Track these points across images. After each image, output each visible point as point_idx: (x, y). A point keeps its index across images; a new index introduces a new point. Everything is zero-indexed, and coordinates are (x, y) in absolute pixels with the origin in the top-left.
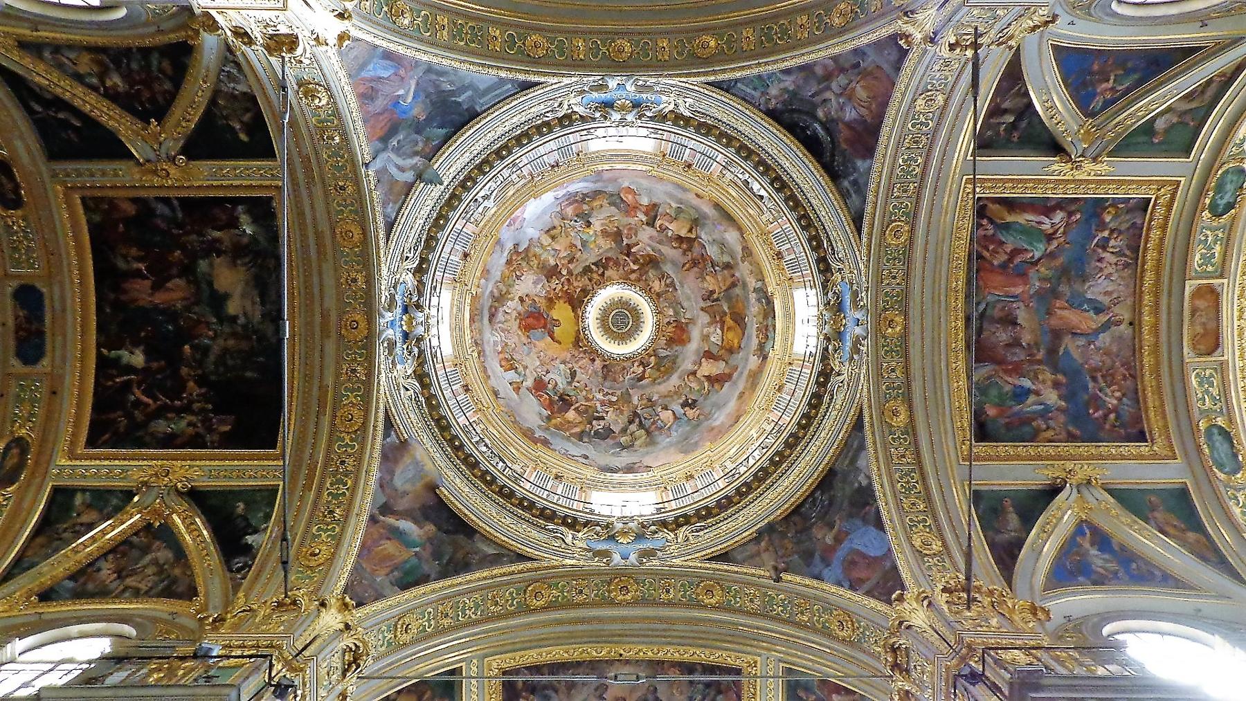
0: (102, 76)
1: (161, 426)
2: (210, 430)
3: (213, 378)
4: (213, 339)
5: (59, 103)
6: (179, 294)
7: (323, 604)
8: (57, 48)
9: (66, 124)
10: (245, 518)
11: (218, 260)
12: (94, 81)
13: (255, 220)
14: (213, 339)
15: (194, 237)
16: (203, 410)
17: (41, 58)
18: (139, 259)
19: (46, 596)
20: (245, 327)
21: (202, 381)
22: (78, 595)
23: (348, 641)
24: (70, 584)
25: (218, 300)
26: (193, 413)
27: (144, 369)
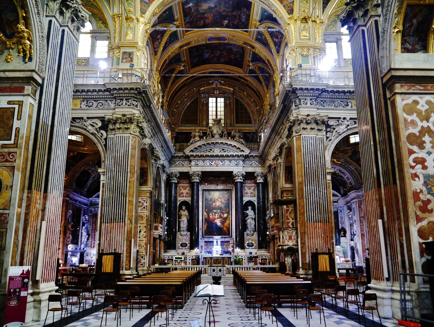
0: (158, 39)
1: (243, 20)
2: (245, 12)
3: (232, 10)
4: (221, 9)
5: (166, 43)
6: (209, 15)
7: (289, 24)
8: (155, 48)
9: (170, 39)
10: (269, 14)
11: (200, 9)
12: (160, 40)
13: (189, 4)
14: (221, 9)
15: (194, 14)
16: (240, 13)
17: (157, 51)
18: (200, 21)
19: (278, 52)
20: (218, 3)
21: (232, 12)
22: (280, 46)
23: (299, 22)
24: (277, 47)
25: (210, 8)
26: (241, 14)
27: (229, 21)
